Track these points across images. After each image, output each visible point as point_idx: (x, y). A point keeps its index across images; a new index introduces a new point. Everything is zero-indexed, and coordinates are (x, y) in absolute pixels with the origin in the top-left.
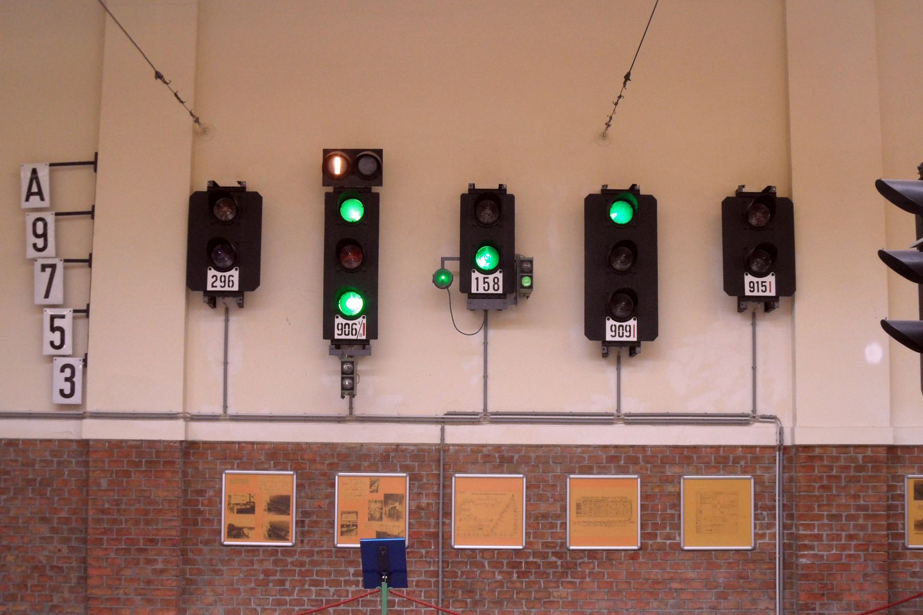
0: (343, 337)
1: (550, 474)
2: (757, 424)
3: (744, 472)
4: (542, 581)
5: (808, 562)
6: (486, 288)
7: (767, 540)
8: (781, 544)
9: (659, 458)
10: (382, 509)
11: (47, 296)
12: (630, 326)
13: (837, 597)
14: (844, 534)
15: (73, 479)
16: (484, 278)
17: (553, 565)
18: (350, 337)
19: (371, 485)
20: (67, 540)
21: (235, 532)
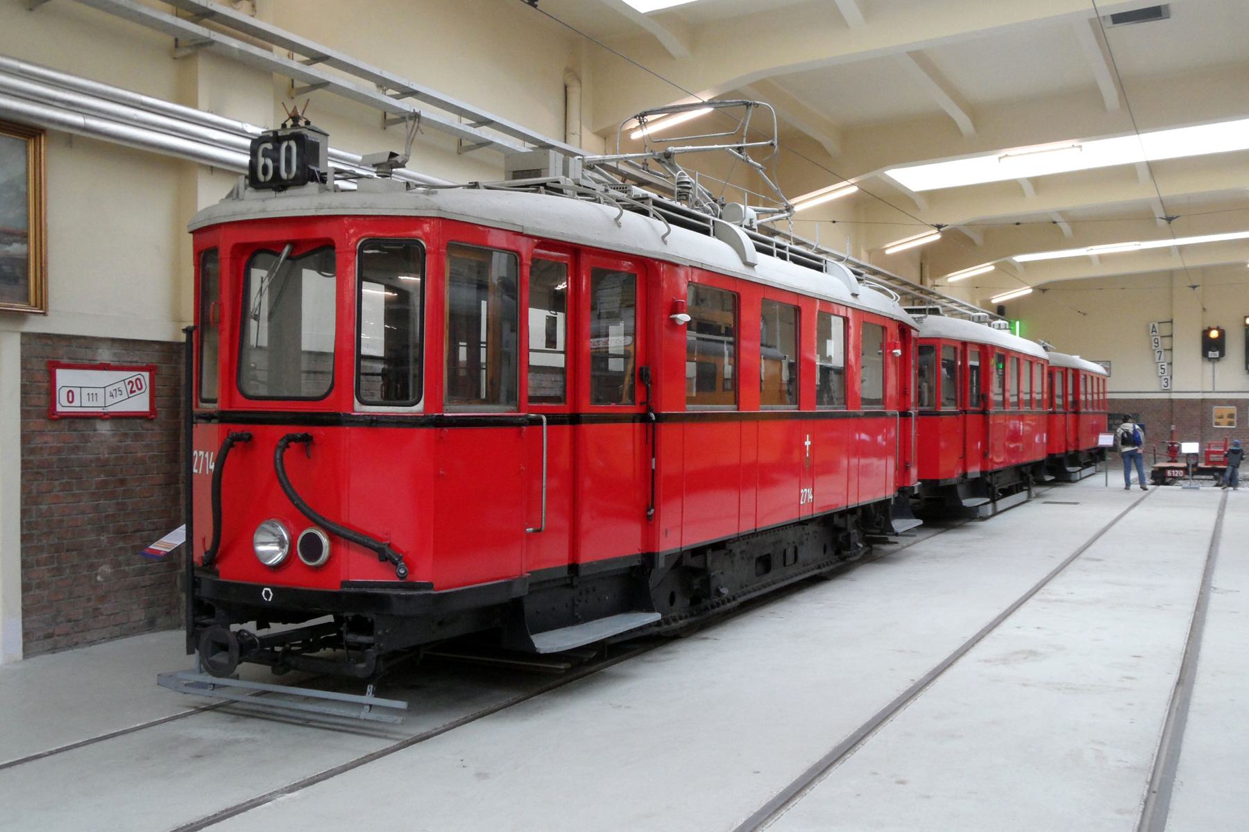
11: (1159, 359)
21: (1217, 424)
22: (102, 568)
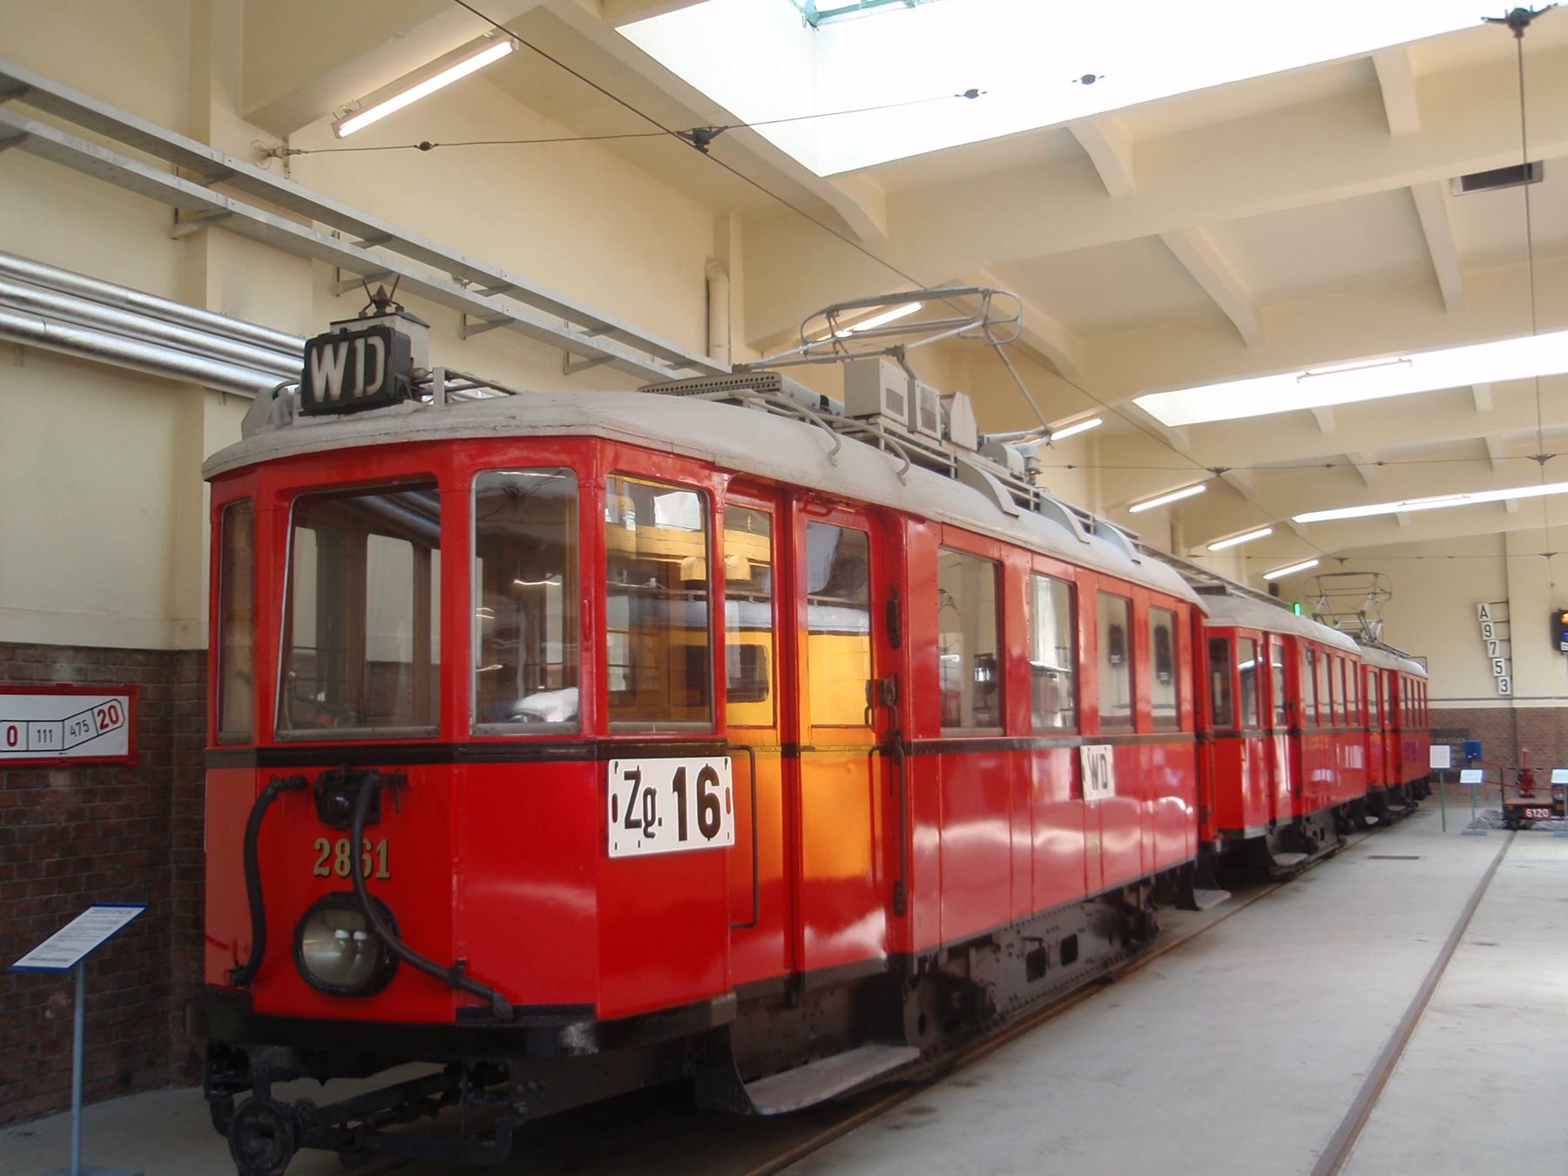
11: (1493, 653)
20: (1507, 746)
22: (52, 998)
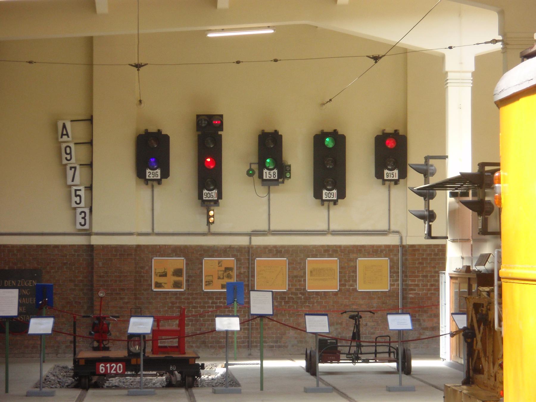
0: (207, 199)
1: (298, 258)
2: (390, 235)
3: (385, 257)
4: (295, 305)
5: (413, 296)
6: (270, 177)
7: (395, 287)
8: (401, 289)
9: (347, 250)
10: (223, 274)
11: (73, 181)
12: (333, 193)
13: (426, 312)
14: (429, 284)
15: (85, 262)
16: (269, 172)
17: (300, 298)
18: (210, 199)
19: (219, 264)
21: (158, 285)
